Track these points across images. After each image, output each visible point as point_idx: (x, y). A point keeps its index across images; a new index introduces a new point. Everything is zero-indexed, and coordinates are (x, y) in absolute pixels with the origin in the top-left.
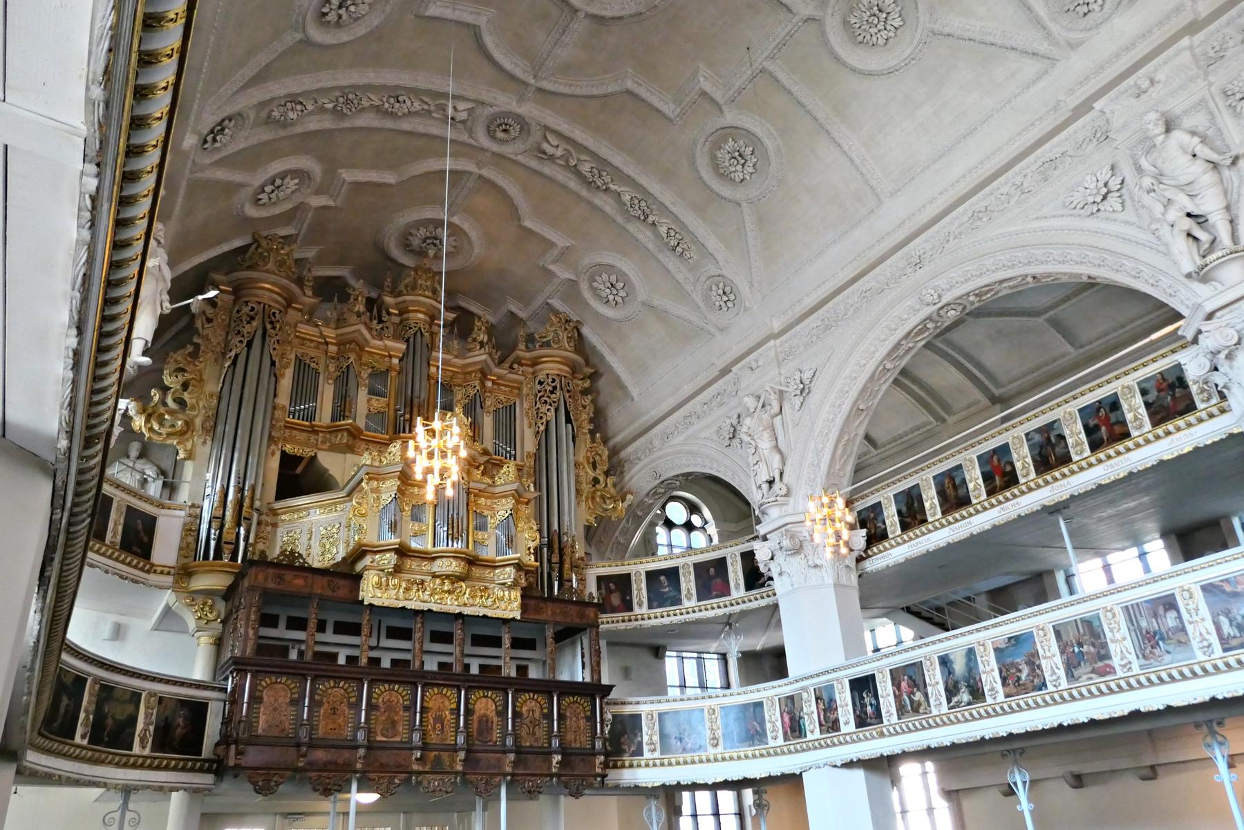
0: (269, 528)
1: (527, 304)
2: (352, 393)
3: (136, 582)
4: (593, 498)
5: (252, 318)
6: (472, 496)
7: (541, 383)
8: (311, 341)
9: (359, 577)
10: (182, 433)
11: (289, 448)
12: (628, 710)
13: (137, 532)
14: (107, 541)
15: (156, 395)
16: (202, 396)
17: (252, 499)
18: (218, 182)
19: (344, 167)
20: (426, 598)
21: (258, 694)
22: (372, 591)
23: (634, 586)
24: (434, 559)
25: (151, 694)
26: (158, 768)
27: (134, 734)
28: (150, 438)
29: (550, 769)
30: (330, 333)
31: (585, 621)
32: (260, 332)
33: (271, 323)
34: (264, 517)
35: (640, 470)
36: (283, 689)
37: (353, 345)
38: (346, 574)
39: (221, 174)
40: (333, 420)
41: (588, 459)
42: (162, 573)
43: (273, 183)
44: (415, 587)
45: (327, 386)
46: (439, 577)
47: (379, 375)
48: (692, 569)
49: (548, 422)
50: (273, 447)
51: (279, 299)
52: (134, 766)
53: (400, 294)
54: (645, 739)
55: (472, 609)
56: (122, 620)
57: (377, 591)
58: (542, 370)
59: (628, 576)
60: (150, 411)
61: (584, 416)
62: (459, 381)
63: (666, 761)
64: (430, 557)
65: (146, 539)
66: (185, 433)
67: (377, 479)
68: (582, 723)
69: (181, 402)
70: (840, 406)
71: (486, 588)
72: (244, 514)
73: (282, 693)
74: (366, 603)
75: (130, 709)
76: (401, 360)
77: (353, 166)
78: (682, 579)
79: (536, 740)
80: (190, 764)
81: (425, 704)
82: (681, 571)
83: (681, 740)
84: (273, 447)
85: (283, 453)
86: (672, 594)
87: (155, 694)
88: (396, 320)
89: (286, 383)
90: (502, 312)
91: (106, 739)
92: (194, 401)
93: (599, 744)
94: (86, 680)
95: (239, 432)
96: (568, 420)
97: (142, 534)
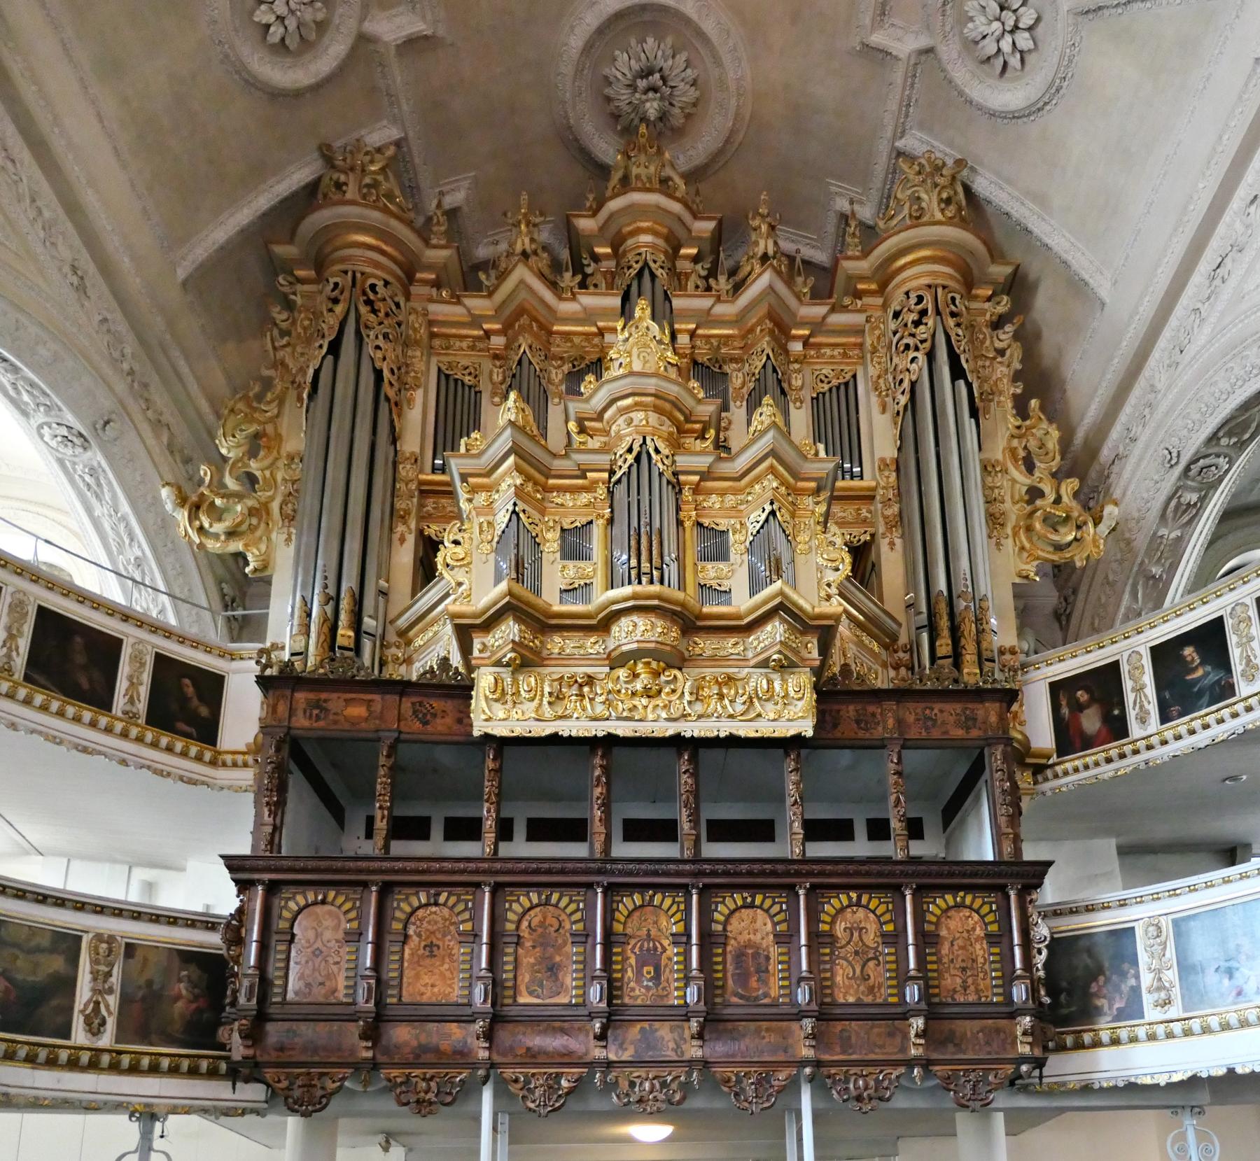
12: (1101, 921)
22: (492, 716)
29: (904, 1049)
30: (478, 304)
37: (524, 320)
49: (913, 384)
54: (1146, 979)
57: (497, 706)
63: (1196, 1025)
68: (980, 949)
79: (871, 990)
83: (1230, 973)
96: (957, 372)
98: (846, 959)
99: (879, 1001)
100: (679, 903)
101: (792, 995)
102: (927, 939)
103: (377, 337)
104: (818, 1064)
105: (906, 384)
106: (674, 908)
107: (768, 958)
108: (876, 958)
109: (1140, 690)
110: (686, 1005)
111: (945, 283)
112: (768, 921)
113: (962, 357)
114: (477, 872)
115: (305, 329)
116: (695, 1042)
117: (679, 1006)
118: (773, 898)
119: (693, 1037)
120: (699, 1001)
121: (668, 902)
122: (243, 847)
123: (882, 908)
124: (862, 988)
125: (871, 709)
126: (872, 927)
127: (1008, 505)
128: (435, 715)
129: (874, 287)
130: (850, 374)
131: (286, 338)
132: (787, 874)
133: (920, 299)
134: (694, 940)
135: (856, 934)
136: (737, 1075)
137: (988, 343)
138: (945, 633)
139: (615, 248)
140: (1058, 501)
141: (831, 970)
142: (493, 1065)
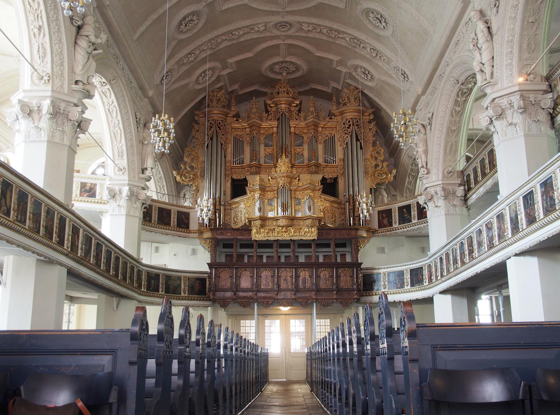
1: (339, 83)
4: (374, 175)
5: (211, 127)
7: (344, 124)
8: (239, 128)
9: (251, 230)
10: (193, 179)
11: (234, 177)
13: (183, 220)
14: (172, 226)
15: (182, 166)
17: (220, 202)
23: (393, 215)
24: (277, 220)
25: (184, 277)
26: (191, 300)
32: (215, 132)
33: (219, 127)
38: (247, 229)
39: (176, 86)
41: (372, 155)
44: (271, 232)
50: (227, 178)
51: (221, 116)
52: (182, 299)
53: (274, 98)
56: (195, 247)
58: (344, 117)
61: (370, 134)
62: (305, 131)
64: (276, 219)
65: (186, 221)
67: (253, 191)
69: (192, 168)
70: (442, 130)
72: (217, 208)
75: (178, 282)
76: (277, 127)
77: (232, 57)
78: (412, 210)
84: (227, 178)
85: (233, 180)
88: (274, 109)
89: (230, 150)
90: (331, 88)
93: (355, 287)
96: (357, 140)
102: (338, 277)
104: (317, 299)
109: (396, 216)
126: (328, 275)
133: (349, 122)
138: (351, 204)
140: (382, 167)
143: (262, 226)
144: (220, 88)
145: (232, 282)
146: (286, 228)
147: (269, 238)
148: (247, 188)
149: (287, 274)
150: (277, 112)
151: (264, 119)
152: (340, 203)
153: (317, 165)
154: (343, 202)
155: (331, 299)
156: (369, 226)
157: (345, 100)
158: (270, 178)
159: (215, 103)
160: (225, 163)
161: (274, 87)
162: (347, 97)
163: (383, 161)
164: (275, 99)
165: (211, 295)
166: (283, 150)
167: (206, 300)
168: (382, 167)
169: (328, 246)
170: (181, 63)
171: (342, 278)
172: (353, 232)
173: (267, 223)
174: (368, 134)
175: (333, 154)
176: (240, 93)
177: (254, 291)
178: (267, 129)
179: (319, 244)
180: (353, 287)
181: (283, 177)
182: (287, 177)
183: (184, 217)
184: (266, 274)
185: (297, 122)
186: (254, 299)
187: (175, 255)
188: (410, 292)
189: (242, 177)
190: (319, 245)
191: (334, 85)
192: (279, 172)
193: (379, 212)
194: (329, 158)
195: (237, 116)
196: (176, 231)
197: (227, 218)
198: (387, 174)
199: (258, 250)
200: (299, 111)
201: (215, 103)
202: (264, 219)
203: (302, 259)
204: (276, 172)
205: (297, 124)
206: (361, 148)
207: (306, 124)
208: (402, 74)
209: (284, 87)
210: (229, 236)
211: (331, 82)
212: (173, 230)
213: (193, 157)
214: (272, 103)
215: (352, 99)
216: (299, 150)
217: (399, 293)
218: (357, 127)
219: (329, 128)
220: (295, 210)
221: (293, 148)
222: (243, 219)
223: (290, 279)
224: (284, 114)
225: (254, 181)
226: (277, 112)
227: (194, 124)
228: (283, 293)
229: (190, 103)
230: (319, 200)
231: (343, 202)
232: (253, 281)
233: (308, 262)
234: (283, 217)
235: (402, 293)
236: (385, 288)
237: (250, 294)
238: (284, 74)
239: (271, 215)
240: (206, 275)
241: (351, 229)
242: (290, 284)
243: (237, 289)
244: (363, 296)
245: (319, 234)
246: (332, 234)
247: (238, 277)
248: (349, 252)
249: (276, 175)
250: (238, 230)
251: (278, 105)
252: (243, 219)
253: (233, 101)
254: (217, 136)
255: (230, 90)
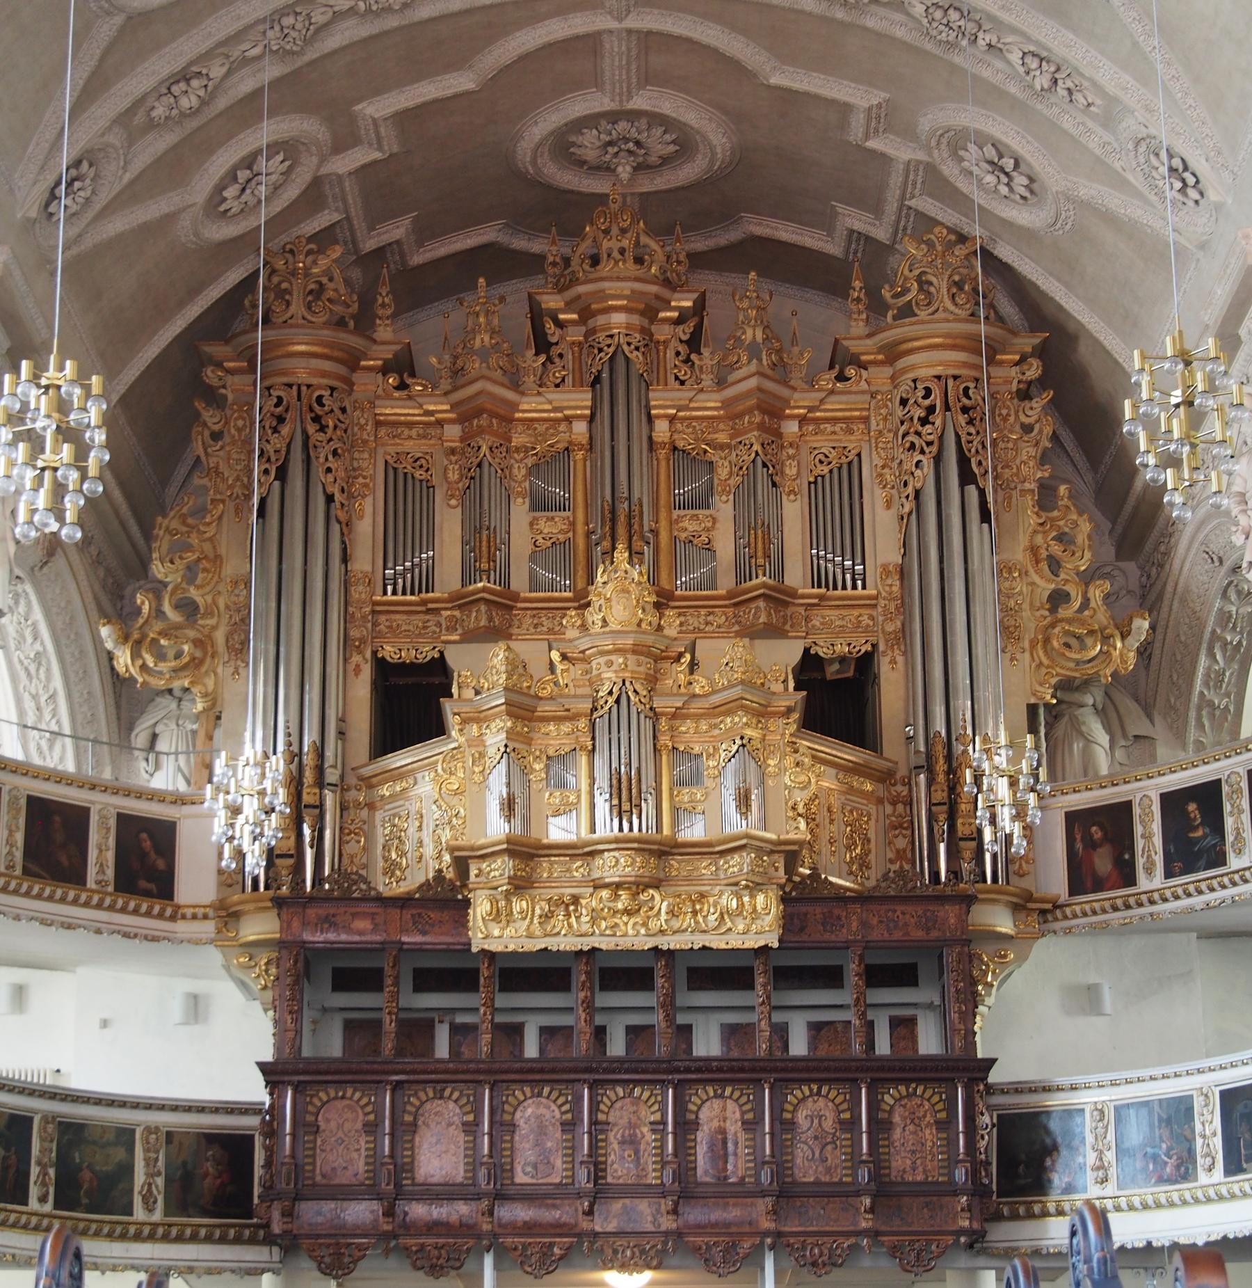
0: (364, 813)
1: (877, 209)
2: (495, 520)
3: (155, 939)
4: (1047, 641)
5: (281, 420)
6: (663, 724)
7: (904, 402)
8: (410, 425)
9: (467, 903)
10: (196, 663)
11: (389, 652)
13: (144, 855)
14: (91, 884)
16: (221, 587)
17: (320, 770)
18: (120, 237)
19: (360, 101)
20: (586, 928)
21: (310, 1118)
23: (1138, 829)
24: (592, 854)
25: (149, 1130)
26: (180, 1239)
27: (132, 1190)
28: (144, 683)
31: (934, 934)
33: (317, 419)
34: (352, 794)
35: (1188, 549)
36: (349, 1107)
37: (484, 420)
38: (446, 899)
39: (117, 225)
40: (467, 579)
41: (1034, 550)
42: (194, 917)
43: (235, 179)
45: (368, 568)
46: (606, 886)
47: (554, 462)
48: (1244, 785)
49: (917, 493)
50: (356, 658)
52: (138, 1237)
53: (574, 282)
55: (677, 937)
57: (492, 925)
58: (904, 371)
59: (1127, 807)
60: (136, 636)
61: (1028, 451)
62: (722, 438)
64: (585, 852)
65: (161, 864)
66: (202, 662)
67: (478, 721)
69: (189, 608)
71: (702, 896)
72: (306, 799)
73: (349, 1115)
74: (474, 949)
75: (120, 1154)
76: (591, 419)
77: (378, 92)
78: (1227, 807)
79: (828, 1170)
80: (247, 1232)
81: (601, 1117)
82: (1225, 789)
84: (356, 658)
85: (382, 667)
86: (1210, 841)
87: (157, 1128)
88: (575, 335)
90: (840, 233)
91: (85, 1201)
92: (209, 598)
93: (960, 1175)
94: (31, 1119)
95: (282, 649)
96: (967, 477)
97: (153, 855)
98: (805, 1143)
99: (836, 1180)
100: (656, 1095)
101: (757, 1175)
102: (880, 1126)
103: (327, 459)
104: (778, 1234)
105: (910, 490)
106: (653, 1100)
107: (736, 1144)
108: (834, 1142)
109: (1150, 836)
110: (662, 1184)
111: (956, 372)
112: (737, 1109)
113: (973, 460)
114: (478, 1071)
115: (239, 430)
116: (670, 1217)
117: (657, 1185)
118: (742, 1090)
119: (668, 1213)
120: (673, 1182)
121: (646, 1094)
122: (268, 1056)
123: (841, 1098)
124: (820, 1169)
125: (836, 912)
127: (1026, 614)
128: (433, 926)
129: (881, 357)
130: (854, 452)
131: (220, 443)
132: (753, 1070)
133: (928, 393)
134: (670, 1128)
135: (816, 1121)
136: (707, 1244)
137: (1012, 419)
138: (941, 778)
139: (583, 320)
140: (1085, 604)
141: (792, 1153)
142: (496, 1236)
143: (520, 885)
144: (323, 239)
145: (374, 1153)
146: (635, 895)
147: (554, 944)
148: (448, 706)
149: (637, 1115)
150: (589, 344)
151: (530, 380)
152: (885, 777)
153: (780, 598)
154: (902, 772)
155: (847, 1234)
156: (1026, 883)
157: (906, 290)
158: (555, 655)
159: (297, 308)
160: (346, 585)
161: (573, 232)
162: (919, 279)
163: (1087, 579)
164: (581, 289)
165: (276, 1215)
166: (617, 525)
167: (252, 1241)
168: (1085, 604)
169: (831, 977)
170: (140, 118)
171: (897, 1134)
172: (950, 914)
173: (545, 869)
174: (1017, 450)
175: (855, 544)
176: (417, 259)
177: (478, 1197)
178: (541, 428)
179: (792, 967)
180: (951, 1175)
181: (618, 651)
182: (637, 650)
183: (147, 844)
184: (536, 1114)
185: (684, 395)
186: (479, 1237)
187: (105, 1024)
188: (1221, 1198)
189: (427, 653)
190: (787, 977)
191: (855, 220)
192: (597, 628)
193: (1072, 818)
194: (834, 563)
195: (403, 368)
196: (111, 908)
197: (350, 848)
198: (1106, 639)
199: (502, 1000)
200: (694, 343)
201: (297, 308)
202: (526, 853)
203: (707, 1044)
204: (584, 627)
205: (682, 406)
206: (985, 516)
207: (726, 404)
208: (1172, 170)
209: (623, 231)
210: (360, 931)
211: (840, 208)
212: (99, 906)
213: (191, 557)
214: (569, 307)
215: (940, 285)
216: (691, 526)
217: (1172, 1205)
218: (962, 419)
219: (835, 420)
220: (675, 810)
221: (663, 515)
222: (429, 850)
223: (650, 1137)
224: (620, 361)
225: (481, 673)
226: (589, 344)
227: (199, 405)
228: (617, 1206)
229: (181, 304)
230: (789, 761)
231: (902, 772)
232: (474, 1146)
233: (735, 1054)
234: (620, 843)
235: (1185, 1203)
236: (1104, 1180)
237: (462, 1210)
238: (624, 171)
239: (560, 830)
240: (254, 1121)
241: (941, 899)
242: (650, 1162)
243: (398, 1185)
244: (998, 1217)
245: (790, 922)
246: (852, 926)
247: (405, 1130)
248: (930, 1006)
249: (584, 643)
250: (403, 902)
251: (594, 314)
252: (429, 850)
253: (384, 296)
254: (308, 461)
255: (369, 245)
